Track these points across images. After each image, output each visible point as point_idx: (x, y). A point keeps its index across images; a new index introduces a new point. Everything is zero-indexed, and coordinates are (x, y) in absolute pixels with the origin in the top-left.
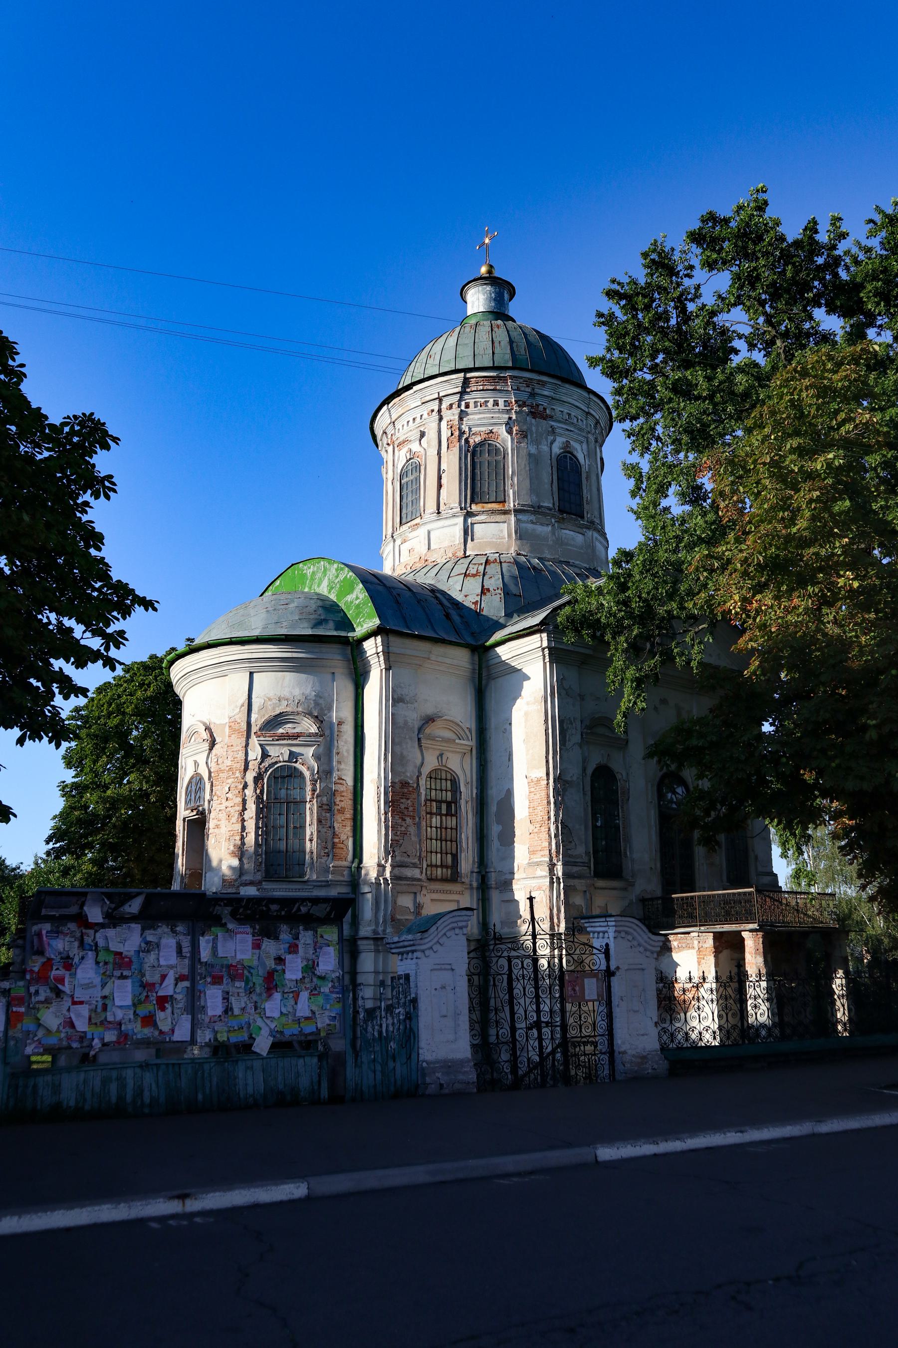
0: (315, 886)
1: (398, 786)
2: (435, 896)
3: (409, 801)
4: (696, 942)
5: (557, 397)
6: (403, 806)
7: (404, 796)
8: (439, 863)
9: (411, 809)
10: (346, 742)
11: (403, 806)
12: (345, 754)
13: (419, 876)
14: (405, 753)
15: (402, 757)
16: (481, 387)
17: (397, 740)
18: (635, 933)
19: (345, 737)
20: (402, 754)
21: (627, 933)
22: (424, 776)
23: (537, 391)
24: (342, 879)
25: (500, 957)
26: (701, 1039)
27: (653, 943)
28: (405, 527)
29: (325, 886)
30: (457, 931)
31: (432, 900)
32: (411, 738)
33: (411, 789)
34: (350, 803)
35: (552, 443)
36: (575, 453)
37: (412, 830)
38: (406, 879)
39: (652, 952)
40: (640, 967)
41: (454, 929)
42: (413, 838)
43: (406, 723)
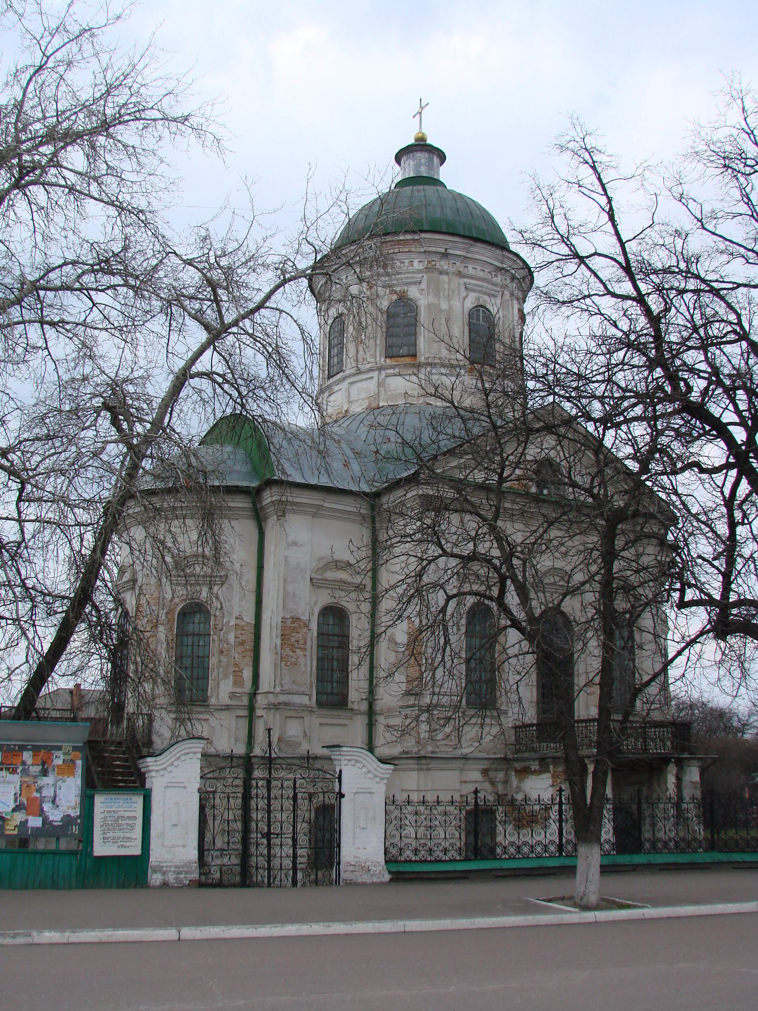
1: (289, 622)
2: (325, 721)
4: (551, 767)
5: (470, 255)
6: (293, 639)
7: (295, 630)
8: (329, 690)
9: (301, 642)
11: (293, 639)
13: (308, 703)
15: (294, 594)
16: (397, 250)
18: (365, 762)
21: (357, 761)
22: (316, 613)
23: (450, 251)
24: (241, 704)
25: (236, 778)
26: (401, 854)
27: (383, 771)
28: (331, 380)
29: (225, 709)
30: (183, 758)
34: (252, 636)
35: (464, 299)
36: (488, 307)
37: (302, 660)
38: (294, 705)
39: (382, 779)
40: (370, 791)
41: (187, 753)
42: (303, 668)
43: (299, 564)
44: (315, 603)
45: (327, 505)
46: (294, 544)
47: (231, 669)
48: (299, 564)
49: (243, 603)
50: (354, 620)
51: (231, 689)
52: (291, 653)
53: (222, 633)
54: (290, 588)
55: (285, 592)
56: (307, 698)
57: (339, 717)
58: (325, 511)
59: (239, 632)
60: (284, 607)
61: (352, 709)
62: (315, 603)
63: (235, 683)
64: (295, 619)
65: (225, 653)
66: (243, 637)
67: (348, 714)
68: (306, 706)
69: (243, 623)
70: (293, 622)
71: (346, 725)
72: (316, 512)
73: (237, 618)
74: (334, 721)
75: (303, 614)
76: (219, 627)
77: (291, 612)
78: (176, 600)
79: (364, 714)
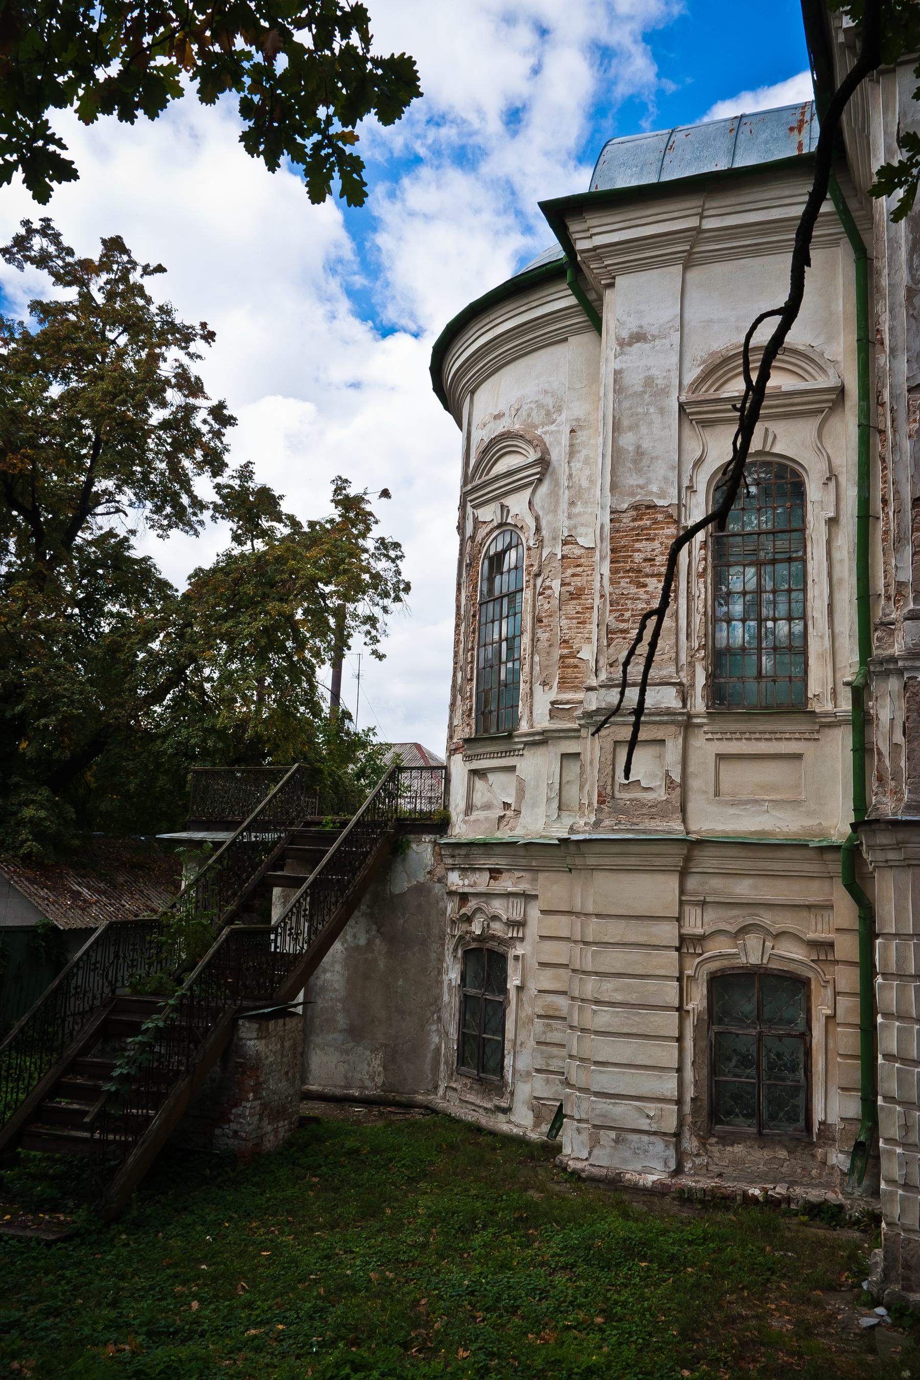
0: (526, 744)
1: (626, 519)
3: (656, 544)
6: (638, 557)
7: (644, 534)
10: (587, 461)
11: (638, 557)
12: (585, 484)
14: (645, 445)
15: (640, 453)
17: (625, 423)
19: (584, 452)
20: (638, 447)
31: (720, 757)
32: (662, 411)
33: (660, 517)
43: (649, 382)
44: (698, 463)
45: (708, 224)
46: (638, 337)
47: (557, 652)
48: (649, 382)
49: (578, 509)
50: (814, 491)
51: (553, 695)
52: (633, 590)
53: (539, 581)
54: (628, 440)
55: (617, 454)
56: (673, 691)
57: (774, 736)
58: (715, 240)
59: (570, 572)
60: (614, 487)
61: (813, 712)
62: (698, 463)
63: (564, 684)
64: (644, 509)
65: (545, 620)
66: (578, 582)
67: (801, 726)
68: (669, 712)
69: (578, 552)
70: (639, 518)
71: (798, 757)
72: (691, 252)
73: (565, 543)
74: (763, 747)
75: (662, 495)
76: (535, 569)
77: (633, 494)
78: (479, 538)
79: (844, 722)
